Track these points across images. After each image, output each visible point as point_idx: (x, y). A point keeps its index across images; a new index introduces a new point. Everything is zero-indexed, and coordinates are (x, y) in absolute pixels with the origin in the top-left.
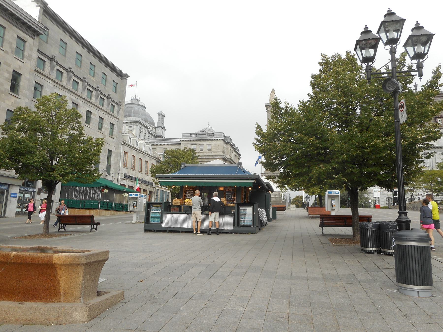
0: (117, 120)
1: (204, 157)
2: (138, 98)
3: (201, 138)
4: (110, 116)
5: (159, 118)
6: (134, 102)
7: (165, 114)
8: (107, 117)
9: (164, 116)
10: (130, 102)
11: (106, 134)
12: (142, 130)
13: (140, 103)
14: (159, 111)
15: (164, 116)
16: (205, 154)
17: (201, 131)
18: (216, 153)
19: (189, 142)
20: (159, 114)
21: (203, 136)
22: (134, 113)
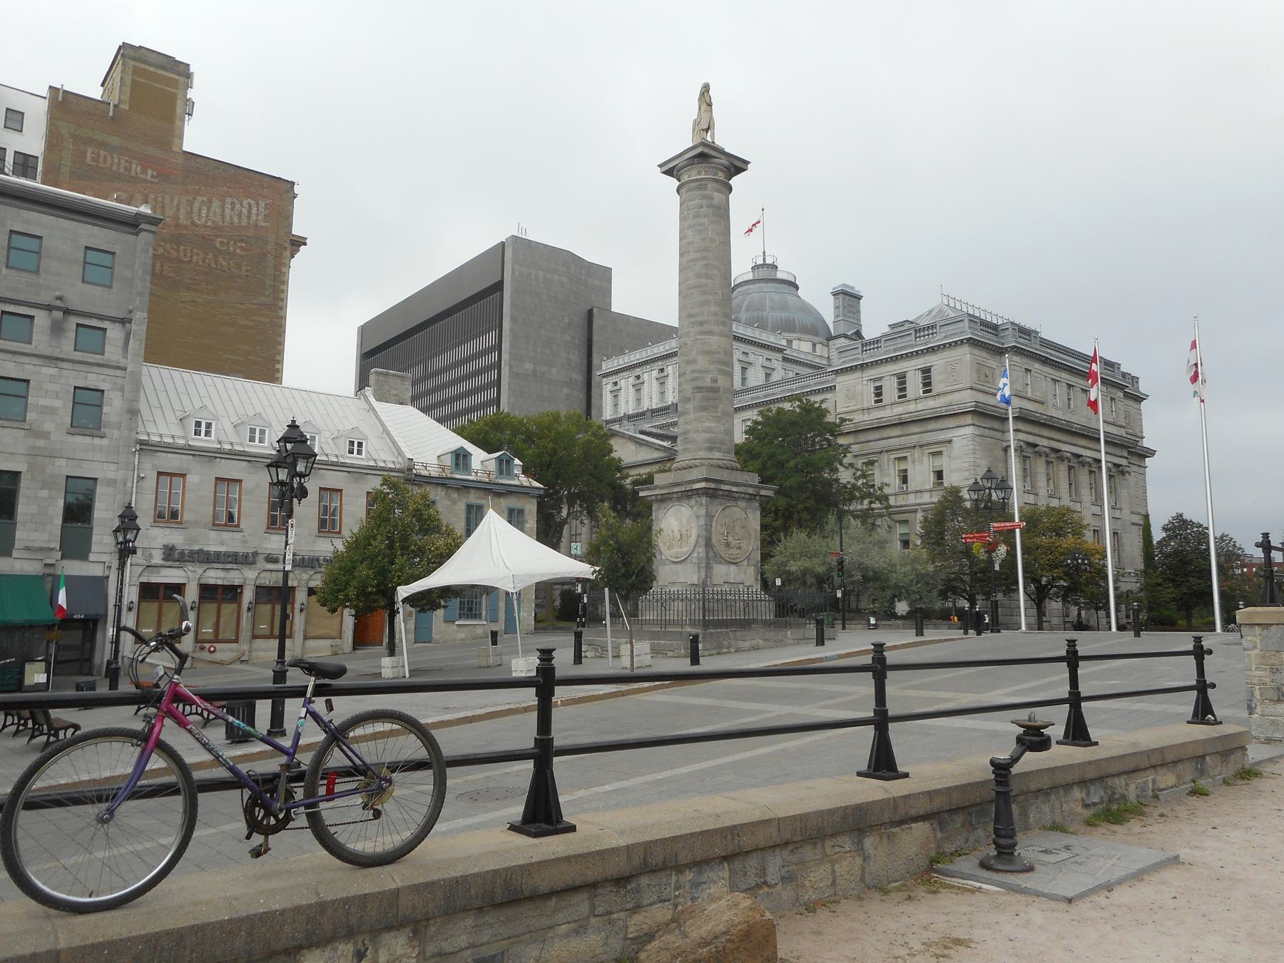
0: (119, 373)
1: (907, 417)
2: (769, 261)
3: (895, 350)
4: (65, 365)
5: (836, 308)
6: (763, 273)
7: (859, 288)
8: (49, 371)
9: (859, 298)
10: (750, 277)
11: (48, 426)
12: (751, 358)
13: (780, 275)
14: (836, 284)
15: (859, 298)
16: (912, 407)
17: (892, 326)
18: (949, 398)
19: (858, 374)
20: (835, 294)
21: (900, 342)
22: (748, 309)
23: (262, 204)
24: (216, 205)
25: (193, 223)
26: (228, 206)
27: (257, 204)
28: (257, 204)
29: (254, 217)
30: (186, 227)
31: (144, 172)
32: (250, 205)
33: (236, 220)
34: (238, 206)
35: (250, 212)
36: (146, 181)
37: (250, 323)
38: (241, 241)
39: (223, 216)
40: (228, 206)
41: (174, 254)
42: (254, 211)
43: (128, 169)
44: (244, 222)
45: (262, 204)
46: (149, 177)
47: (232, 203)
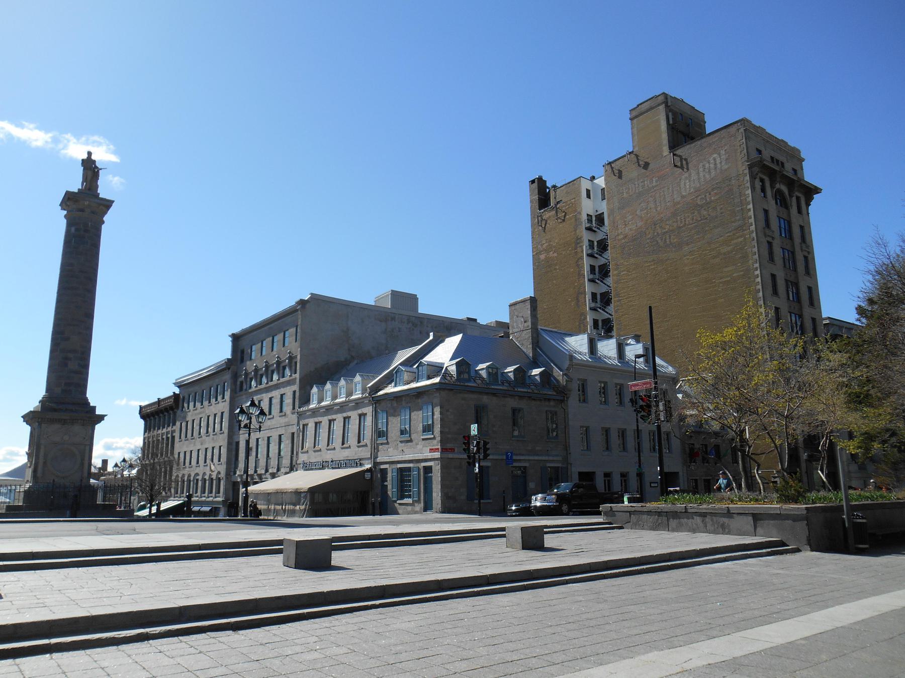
23: (723, 152)
24: (694, 176)
25: (683, 197)
26: (701, 170)
27: (719, 154)
28: (719, 154)
29: (719, 166)
30: (679, 203)
31: (652, 182)
32: (715, 159)
33: (707, 176)
34: (707, 165)
35: (715, 164)
36: (653, 187)
37: (729, 248)
38: (713, 189)
39: (699, 179)
40: (701, 170)
41: (675, 225)
42: (718, 161)
43: (643, 186)
44: (713, 173)
45: (723, 152)
46: (654, 184)
47: (704, 166)
